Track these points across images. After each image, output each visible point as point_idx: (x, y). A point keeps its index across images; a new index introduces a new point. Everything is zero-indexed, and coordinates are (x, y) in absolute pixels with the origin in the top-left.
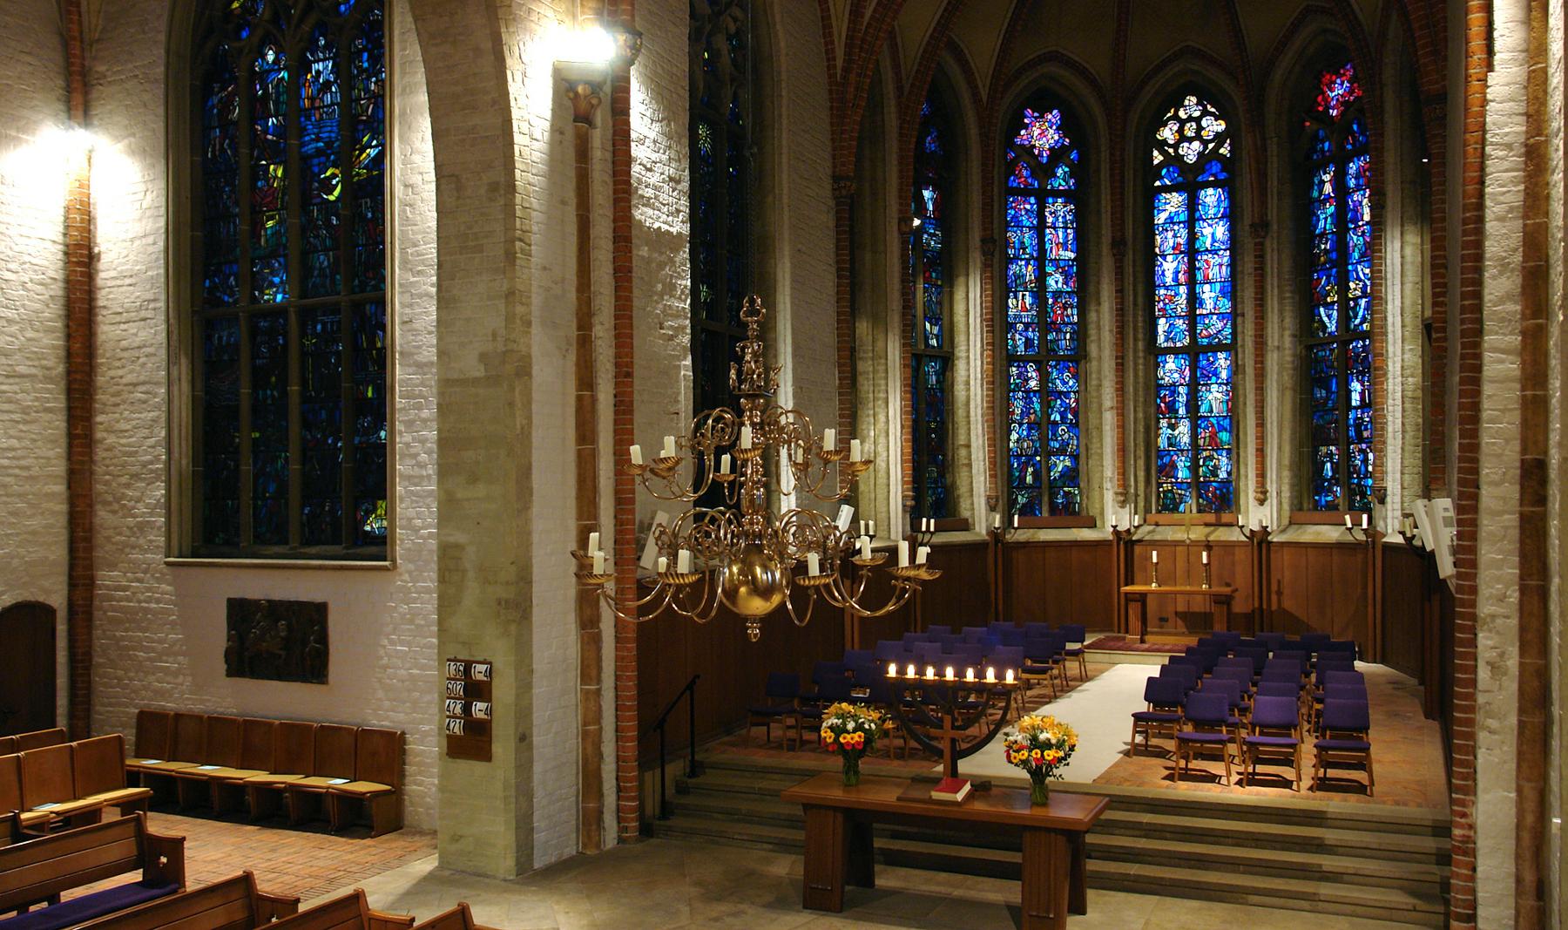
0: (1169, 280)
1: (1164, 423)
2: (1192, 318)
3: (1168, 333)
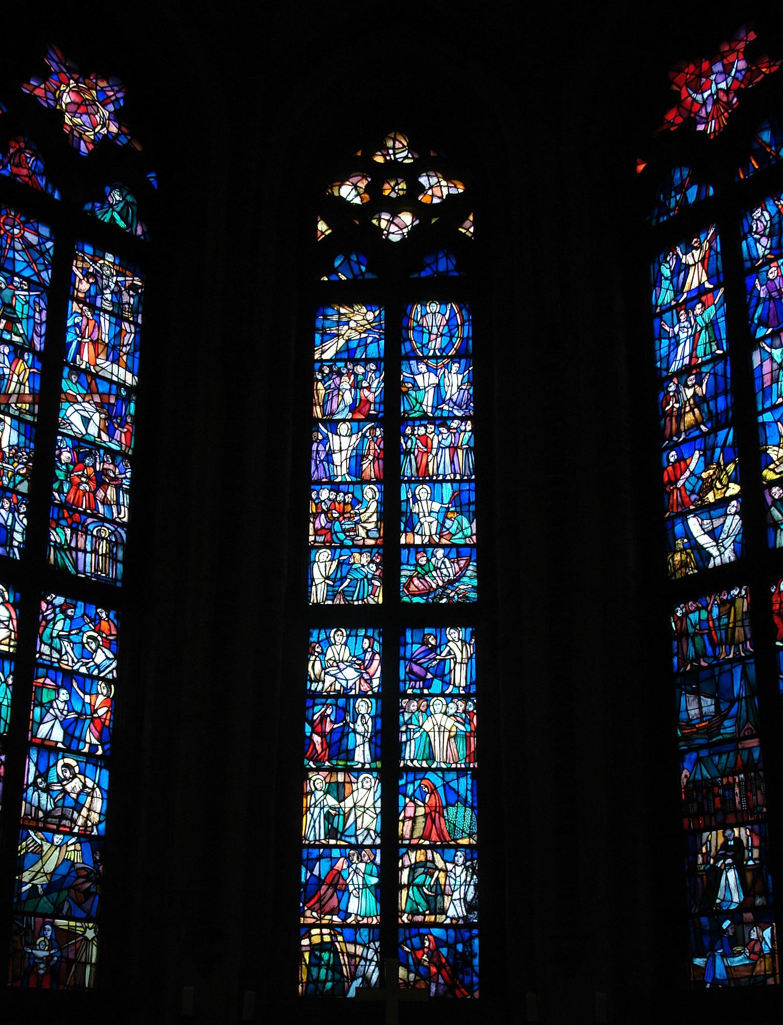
0: (341, 468)
1: (317, 780)
2: (390, 553)
3: (334, 580)
